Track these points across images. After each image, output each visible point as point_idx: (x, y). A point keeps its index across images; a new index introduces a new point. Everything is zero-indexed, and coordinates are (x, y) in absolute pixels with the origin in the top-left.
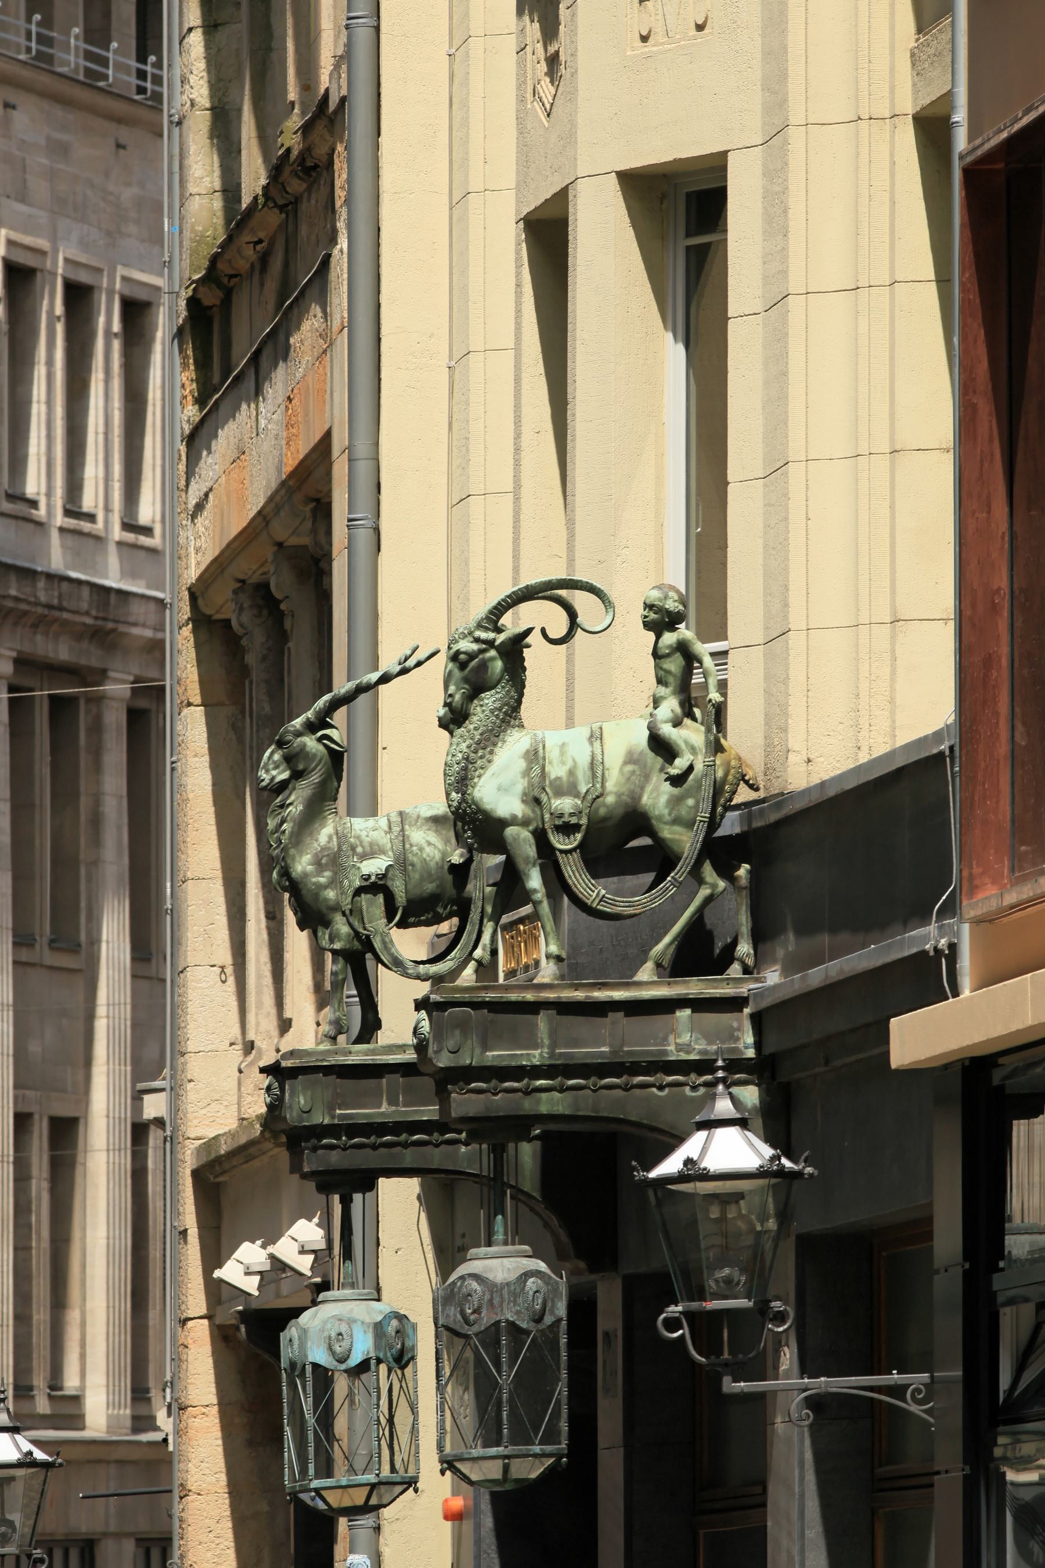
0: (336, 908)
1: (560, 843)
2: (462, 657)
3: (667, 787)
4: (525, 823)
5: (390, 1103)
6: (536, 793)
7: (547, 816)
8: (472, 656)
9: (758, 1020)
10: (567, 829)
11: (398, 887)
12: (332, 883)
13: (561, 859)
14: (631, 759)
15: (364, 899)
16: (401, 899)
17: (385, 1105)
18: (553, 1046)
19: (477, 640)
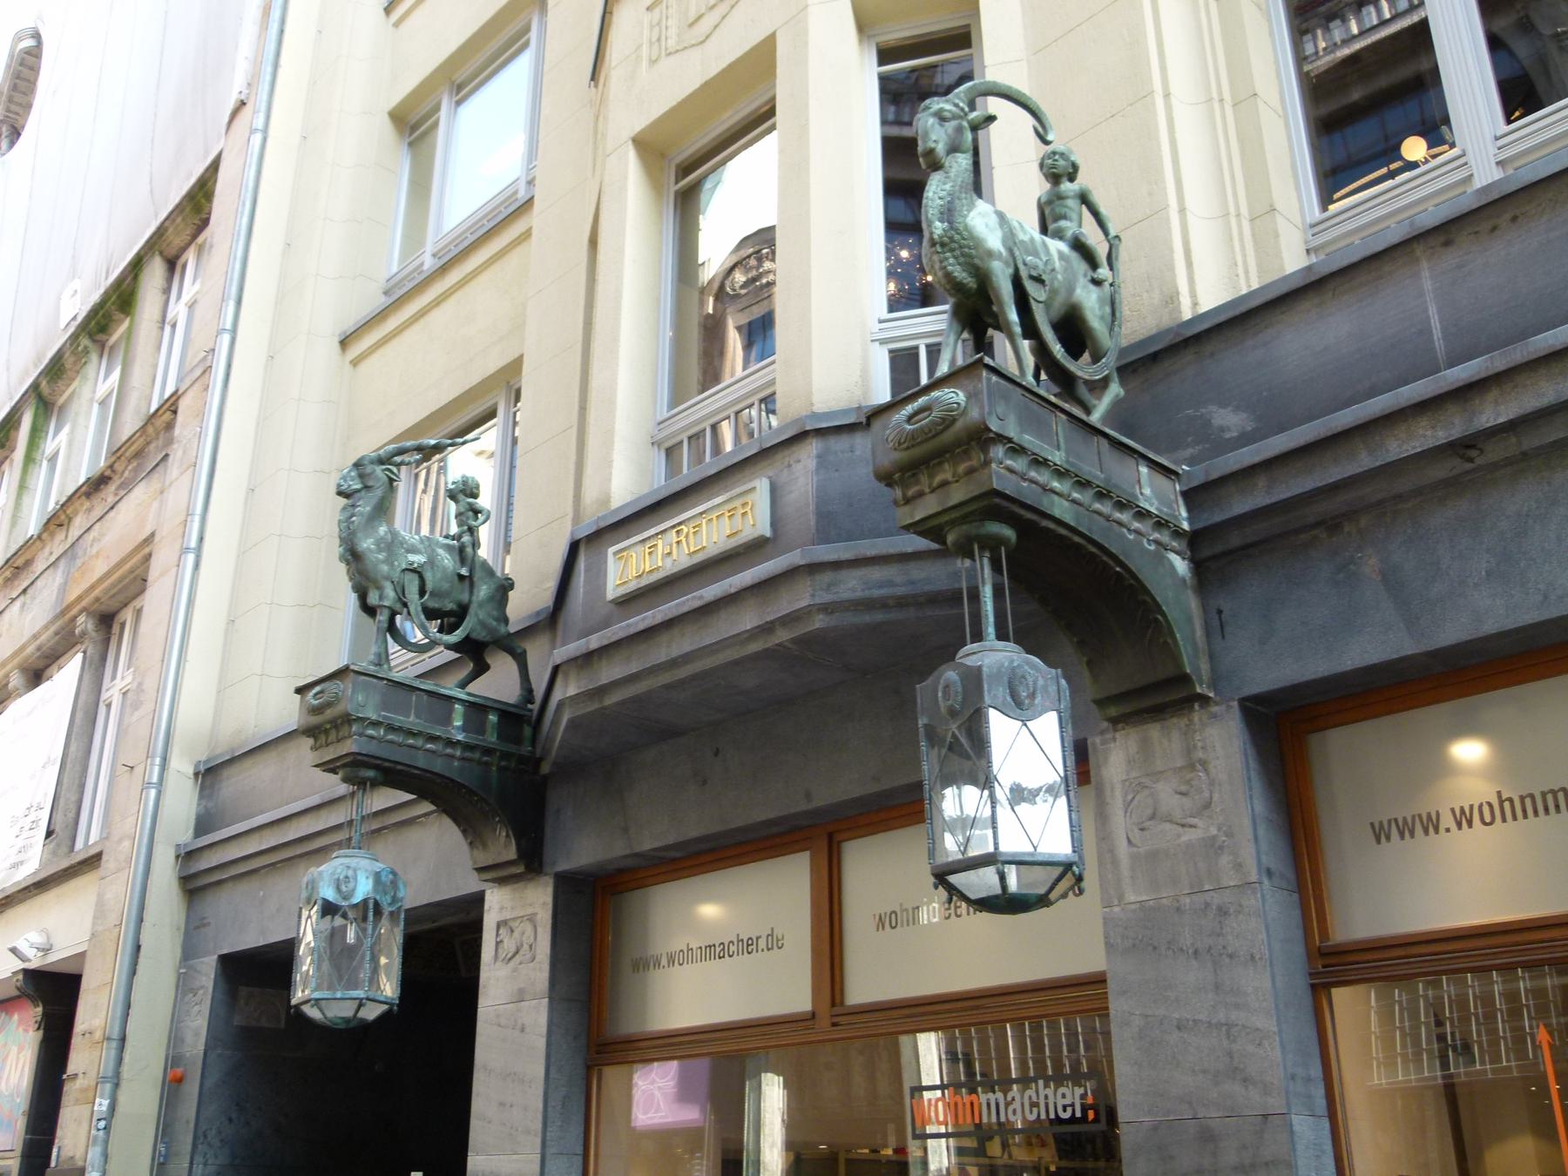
0: (387, 578)
1: (1030, 287)
2: (947, 114)
3: (1092, 287)
4: (1007, 264)
5: (417, 716)
6: (1010, 243)
7: (1021, 267)
8: (955, 117)
9: (1188, 495)
10: (1038, 280)
11: (428, 576)
12: (386, 561)
13: (1034, 305)
14: (1061, 256)
15: (409, 577)
16: (429, 586)
17: (412, 718)
18: (1068, 452)
19: (956, 105)
